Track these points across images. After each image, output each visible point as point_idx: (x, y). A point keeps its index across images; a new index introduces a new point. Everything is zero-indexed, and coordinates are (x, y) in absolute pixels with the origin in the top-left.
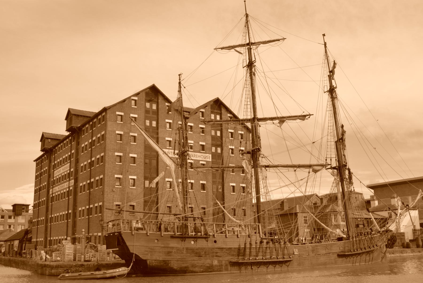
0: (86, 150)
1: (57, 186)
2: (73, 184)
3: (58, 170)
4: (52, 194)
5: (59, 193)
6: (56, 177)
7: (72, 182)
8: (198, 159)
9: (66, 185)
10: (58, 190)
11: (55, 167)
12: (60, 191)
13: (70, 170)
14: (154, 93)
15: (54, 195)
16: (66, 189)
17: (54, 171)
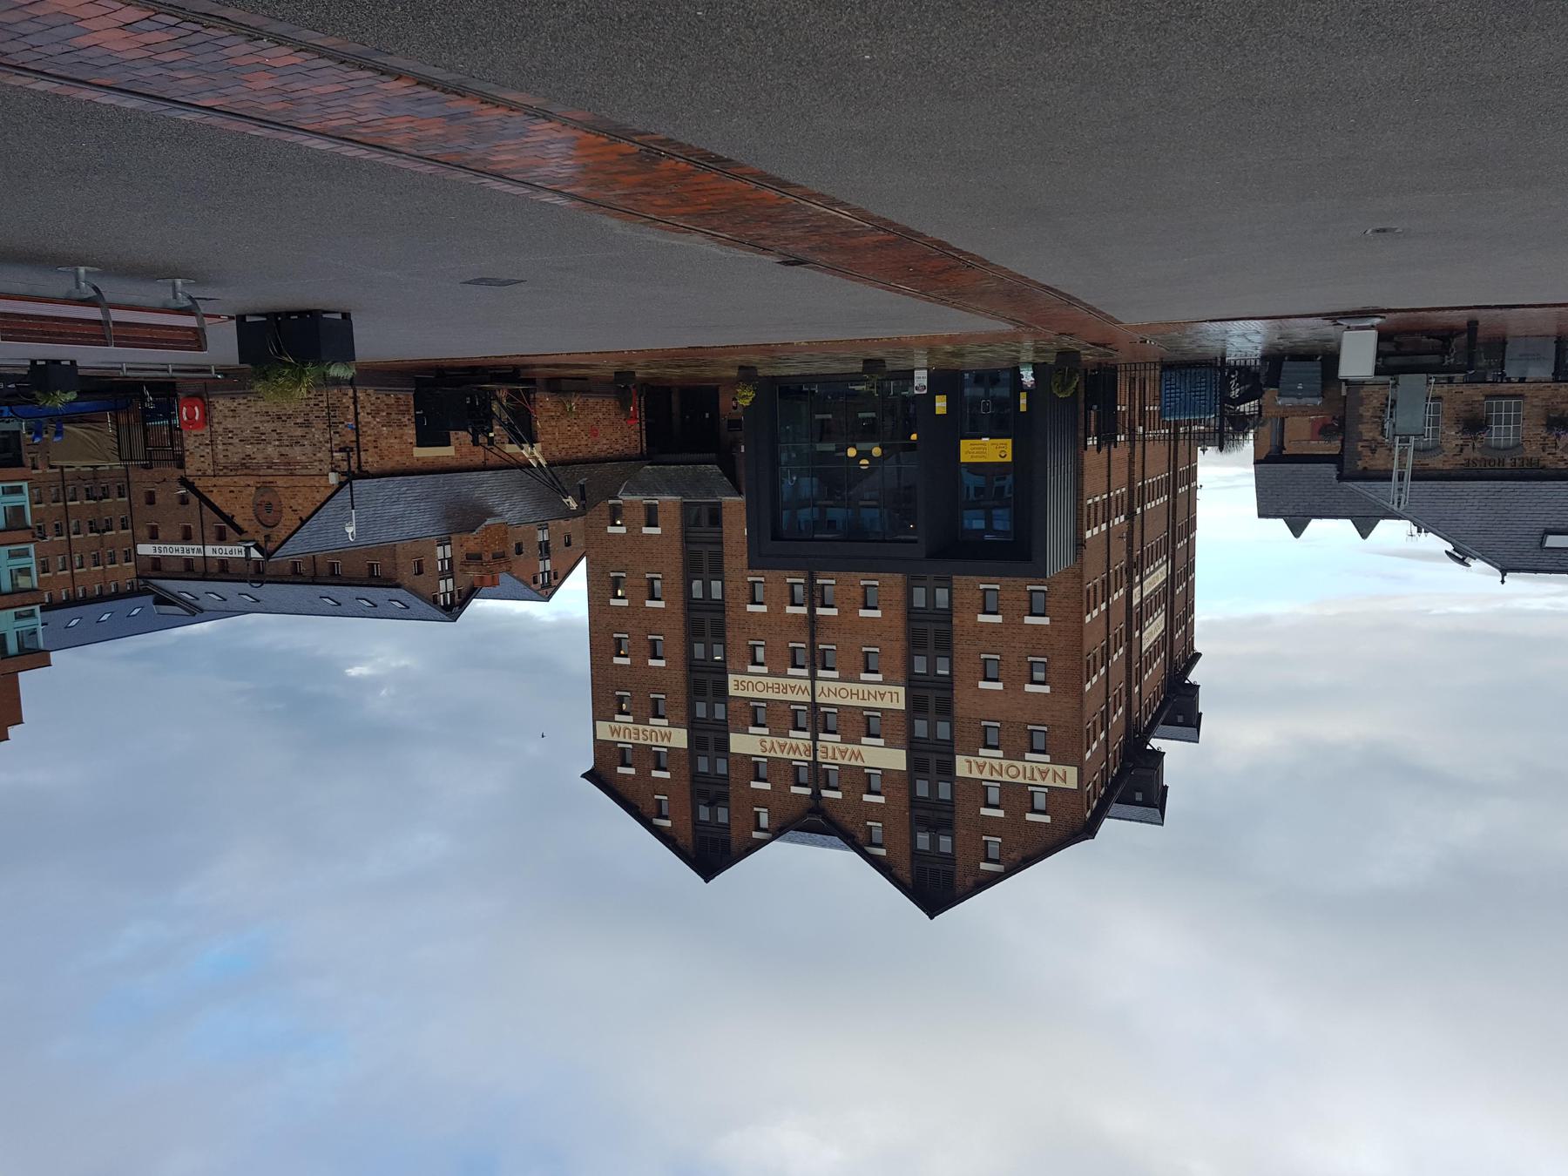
8: (770, 681)
14: (934, 888)
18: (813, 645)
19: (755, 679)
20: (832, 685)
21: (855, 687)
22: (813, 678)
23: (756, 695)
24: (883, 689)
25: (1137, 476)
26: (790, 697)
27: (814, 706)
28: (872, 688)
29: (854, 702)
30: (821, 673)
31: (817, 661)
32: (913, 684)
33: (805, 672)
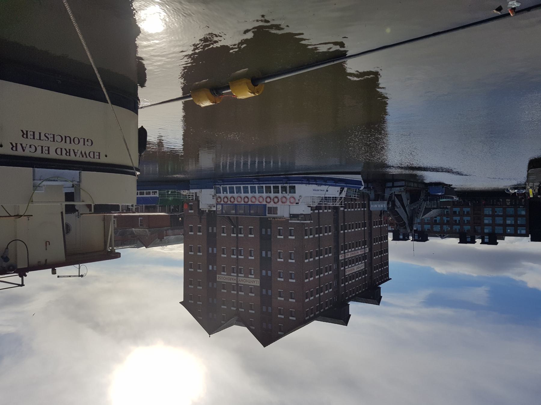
1: (360, 255)
2: (340, 256)
3: (358, 270)
4: (365, 248)
5: (357, 248)
6: (362, 263)
7: (341, 257)
9: (349, 255)
10: (359, 251)
11: (363, 272)
12: (355, 250)
13: (345, 269)
15: (363, 247)
16: (348, 252)
17: (365, 269)
18: (237, 267)
19: (223, 276)
20: (242, 278)
21: (248, 279)
22: (237, 276)
26: (232, 281)
27: (237, 284)
30: (240, 275)
31: (239, 271)
33: (235, 275)
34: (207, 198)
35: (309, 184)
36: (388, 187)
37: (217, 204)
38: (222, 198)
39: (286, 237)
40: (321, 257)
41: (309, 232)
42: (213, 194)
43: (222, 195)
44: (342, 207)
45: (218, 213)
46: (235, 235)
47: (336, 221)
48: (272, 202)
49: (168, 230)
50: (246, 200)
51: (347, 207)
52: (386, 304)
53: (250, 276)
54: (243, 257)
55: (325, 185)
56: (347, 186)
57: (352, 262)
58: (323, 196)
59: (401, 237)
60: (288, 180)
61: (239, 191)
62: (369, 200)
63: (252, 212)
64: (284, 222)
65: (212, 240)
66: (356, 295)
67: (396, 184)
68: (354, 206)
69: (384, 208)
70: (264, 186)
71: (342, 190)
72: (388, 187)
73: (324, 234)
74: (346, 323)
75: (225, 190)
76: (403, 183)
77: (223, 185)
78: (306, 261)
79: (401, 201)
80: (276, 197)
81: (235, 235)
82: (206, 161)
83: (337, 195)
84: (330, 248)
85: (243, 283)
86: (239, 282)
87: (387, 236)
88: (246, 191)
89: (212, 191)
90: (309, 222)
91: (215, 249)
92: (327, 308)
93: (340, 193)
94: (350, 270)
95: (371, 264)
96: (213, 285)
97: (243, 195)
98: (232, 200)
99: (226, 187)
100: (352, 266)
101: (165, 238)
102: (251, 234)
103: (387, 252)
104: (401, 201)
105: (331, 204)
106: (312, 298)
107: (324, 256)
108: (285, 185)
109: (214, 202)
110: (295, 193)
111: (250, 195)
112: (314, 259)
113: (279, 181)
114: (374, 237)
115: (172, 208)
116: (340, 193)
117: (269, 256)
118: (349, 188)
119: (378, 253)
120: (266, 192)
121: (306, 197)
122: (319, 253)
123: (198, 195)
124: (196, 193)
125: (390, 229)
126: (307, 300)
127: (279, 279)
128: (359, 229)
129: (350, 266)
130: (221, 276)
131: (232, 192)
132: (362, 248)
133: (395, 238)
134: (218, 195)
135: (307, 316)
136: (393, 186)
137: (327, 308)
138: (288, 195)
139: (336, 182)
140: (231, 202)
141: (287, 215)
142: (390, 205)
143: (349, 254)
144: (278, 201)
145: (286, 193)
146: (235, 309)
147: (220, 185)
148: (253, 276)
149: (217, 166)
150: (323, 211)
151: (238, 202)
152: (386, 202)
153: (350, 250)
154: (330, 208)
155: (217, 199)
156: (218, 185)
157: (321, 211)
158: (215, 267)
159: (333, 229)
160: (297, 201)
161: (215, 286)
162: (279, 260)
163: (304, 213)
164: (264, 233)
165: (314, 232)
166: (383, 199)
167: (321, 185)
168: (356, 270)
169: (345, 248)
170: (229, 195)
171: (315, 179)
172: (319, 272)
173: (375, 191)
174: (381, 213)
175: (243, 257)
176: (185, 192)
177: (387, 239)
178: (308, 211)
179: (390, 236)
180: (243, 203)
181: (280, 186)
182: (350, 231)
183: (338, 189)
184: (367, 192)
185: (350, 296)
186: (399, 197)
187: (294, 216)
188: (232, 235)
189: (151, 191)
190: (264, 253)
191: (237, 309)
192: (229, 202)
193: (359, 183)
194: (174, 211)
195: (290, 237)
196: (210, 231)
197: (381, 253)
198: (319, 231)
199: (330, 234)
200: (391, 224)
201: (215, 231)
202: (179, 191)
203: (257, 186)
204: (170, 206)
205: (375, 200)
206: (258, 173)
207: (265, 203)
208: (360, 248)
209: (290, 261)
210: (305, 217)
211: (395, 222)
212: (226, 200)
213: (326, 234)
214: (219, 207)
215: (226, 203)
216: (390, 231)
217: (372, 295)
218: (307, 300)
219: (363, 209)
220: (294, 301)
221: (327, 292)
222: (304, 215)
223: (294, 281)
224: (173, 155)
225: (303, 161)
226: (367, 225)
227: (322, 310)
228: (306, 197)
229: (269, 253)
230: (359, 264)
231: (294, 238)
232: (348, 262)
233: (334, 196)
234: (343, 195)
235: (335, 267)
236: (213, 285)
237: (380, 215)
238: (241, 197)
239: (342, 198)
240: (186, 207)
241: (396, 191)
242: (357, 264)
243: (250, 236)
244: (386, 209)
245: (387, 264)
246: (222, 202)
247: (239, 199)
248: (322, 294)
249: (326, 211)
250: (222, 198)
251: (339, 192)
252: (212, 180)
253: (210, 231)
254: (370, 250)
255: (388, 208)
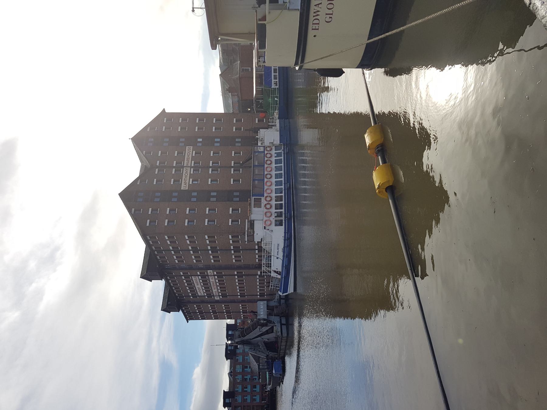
0: (181, 257)
1: (212, 291)
4: (219, 296)
5: (219, 288)
9: (212, 280)
11: (195, 295)
12: (217, 286)
13: (198, 276)
15: (220, 294)
16: (215, 279)
19: (191, 153)
20: (189, 172)
22: (191, 167)
23: (186, 153)
24: (187, 184)
25: (254, 297)
26: (186, 161)
27: (183, 167)
28: (187, 182)
29: (184, 177)
30: (192, 169)
31: (196, 169)
32: (188, 192)
33: (193, 165)
34: (270, 136)
35: (285, 240)
36: (281, 320)
37: (264, 147)
38: (270, 152)
39: (230, 216)
40: (210, 252)
41: (235, 239)
42: (274, 143)
43: (273, 152)
44: (261, 273)
45: (255, 147)
46: (233, 165)
47: (247, 267)
48: (266, 202)
49: (238, 97)
50: (269, 176)
51: (261, 278)
52: (163, 319)
53: (191, 180)
54: (210, 172)
55: (283, 256)
56: (282, 278)
57: (205, 283)
58: (272, 254)
59: (230, 333)
60: (289, 219)
61: (277, 169)
62: (268, 301)
63: (256, 182)
64: (246, 214)
65: (228, 141)
66: (171, 287)
67: (284, 327)
68: (261, 285)
69: (260, 315)
70: (283, 194)
71: (278, 273)
72: (281, 320)
73: (233, 254)
74: (143, 276)
75: (279, 155)
76: (285, 335)
77: (284, 153)
78: (206, 237)
79: (267, 332)
80: (271, 207)
81: (233, 165)
82: (307, 136)
83: (273, 268)
84: (219, 261)
85: (184, 173)
86: (185, 169)
87: (231, 318)
88: (277, 176)
89: (277, 142)
90: (246, 240)
91: (218, 144)
92: (159, 258)
93: (275, 271)
94: (197, 282)
95: (203, 302)
96: (182, 142)
97: (274, 173)
98: (269, 162)
99: (281, 156)
100: (200, 283)
101: (230, 94)
102: (234, 181)
103: (215, 319)
104: (267, 332)
105: (264, 261)
106: (168, 242)
107: (211, 255)
108: (283, 215)
109: (267, 143)
110: (276, 225)
111: (274, 180)
112: (208, 245)
113: (288, 210)
114: (230, 304)
115: (261, 101)
116: (275, 271)
117: (212, 199)
118: (280, 280)
119: (213, 310)
120: (276, 197)
121: (272, 237)
122: (214, 250)
123: (273, 127)
124: (275, 125)
125: (239, 321)
126: (167, 238)
127: (188, 209)
128: (238, 291)
129: (201, 281)
130: (191, 151)
131: (277, 162)
132: (219, 293)
133: (229, 327)
134: (274, 147)
135: (150, 237)
136: (282, 325)
137: (159, 258)
138: (273, 219)
139: (286, 267)
140: (267, 161)
141: (253, 217)
142: (262, 322)
143: (213, 280)
144: (267, 208)
145: (275, 217)
146: (158, 164)
147: (284, 150)
148: (191, 183)
149: (303, 147)
150: (257, 254)
151: (267, 168)
152: (266, 317)
153: (217, 281)
154: (260, 260)
155: (269, 147)
156: (284, 148)
157: (257, 251)
158: (200, 144)
159: (238, 263)
160: (267, 228)
161: (181, 144)
162: (207, 209)
163: (255, 234)
164: (235, 194)
165: (236, 244)
166: (269, 314)
167: (284, 252)
168: (196, 286)
169: (220, 276)
170: (273, 159)
171: (289, 246)
172: (195, 250)
173: (277, 307)
174: (254, 312)
175: (210, 172)
176: (276, 115)
177: (228, 319)
178: (257, 239)
179: (231, 322)
180: (266, 173)
181: (283, 210)
182: (237, 281)
183: (280, 270)
184: (276, 298)
185: (170, 281)
186: (271, 330)
187: (252, 224)
188: (233, 162)
189: (277, 80)
190: (215, 194)
191: (157, 167)
192: (266, 159)
193: (285, 290)
194: (258, 103)
195: (230, 220)
196: (237, 140)
197: (214, 312)
198: (237, 249)
199: (234, 261)
200: (243, 322)
201: (237, 144)
202: (277, 108)
203: (283, 187)
204: (262, 99)
205: (267, 305)
206: (296, 188)
207: (265, 195)
208: (219, 291)
209: (207, 220)
210: (251, 236)
211: (246, 327)
212: (269, 156)
213: (233, 257)
214: (262, 149)
215: (265, 156)
216: (236, 321)
217: (171, 303)
218: (166, 237)
219: (258, 294)
220: (166, 224)
221: (175, 257)
222: (253, 235)
223: (186, 224)
224: (314, 103)
225: (308, 234)
226: (243, 298)
227: (156, 253)
228: (272, 237)
229: (215, 199)
230: (203, 290)
231: (230, 224)
232: (204, 279)
233: (272, 265)
234: (273, 274)
235: (201, 265)
236: (182, 142)
237: (252, 312)
238: (271, 171)
239: (270, 273)
240: (261, 115)
241: (277, 328)
242: (203, 288)
243: (232, 180)
244: (258, 317)
245: (203, 318)
246: (266, 152)
247: (269, 169)
248: (173, 252)
249: (257, 256)
250: (270, 152)
251: (277, 270)
252: (289, 141)
253: (237, 140)
254: (217, 302)
255: (259, 319)
